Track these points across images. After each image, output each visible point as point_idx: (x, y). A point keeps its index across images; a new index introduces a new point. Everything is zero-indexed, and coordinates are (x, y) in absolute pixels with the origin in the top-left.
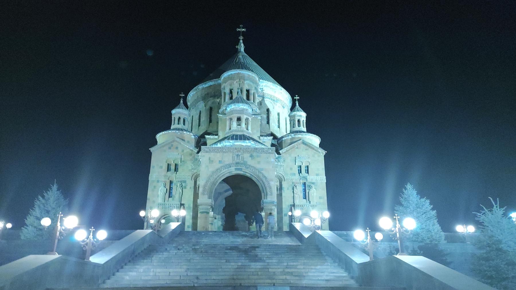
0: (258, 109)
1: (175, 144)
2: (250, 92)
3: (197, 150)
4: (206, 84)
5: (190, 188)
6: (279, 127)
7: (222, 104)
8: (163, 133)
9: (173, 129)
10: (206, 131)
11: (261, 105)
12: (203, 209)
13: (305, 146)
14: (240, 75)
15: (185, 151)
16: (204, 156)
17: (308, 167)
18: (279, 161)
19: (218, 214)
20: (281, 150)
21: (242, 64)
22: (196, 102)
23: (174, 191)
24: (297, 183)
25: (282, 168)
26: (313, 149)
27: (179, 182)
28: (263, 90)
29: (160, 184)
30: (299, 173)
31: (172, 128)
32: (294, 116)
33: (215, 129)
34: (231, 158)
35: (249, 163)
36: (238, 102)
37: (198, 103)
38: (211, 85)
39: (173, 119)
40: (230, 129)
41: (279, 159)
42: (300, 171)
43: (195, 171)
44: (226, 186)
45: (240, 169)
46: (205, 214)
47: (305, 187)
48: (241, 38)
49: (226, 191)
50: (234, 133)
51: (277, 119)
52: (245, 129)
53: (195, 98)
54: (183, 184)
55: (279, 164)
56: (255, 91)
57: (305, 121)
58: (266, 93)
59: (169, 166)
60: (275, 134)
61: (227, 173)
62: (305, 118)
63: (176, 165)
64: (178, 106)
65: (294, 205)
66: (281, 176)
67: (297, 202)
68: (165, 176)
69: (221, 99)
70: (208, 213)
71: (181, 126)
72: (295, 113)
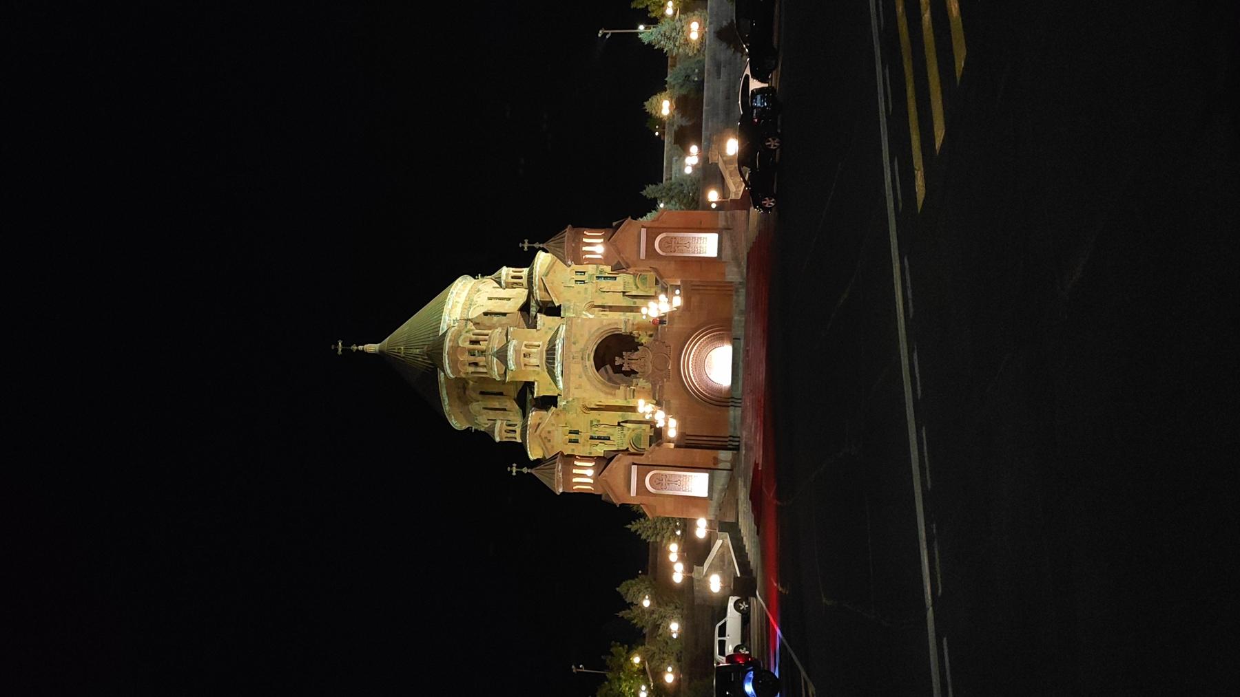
0: (496, 330)
1: (543, 435)
3: (552, 407)
4: (444, 400)
6: (509, 299)
9: (523, 435)
10: (515, 400)
11: (479, 324)
12: (630, 395)
15: (553, 422)
16: (573, 395)
17: (576, 272)
18: (569, 307)
19: (632, 382)
20: (554, 303)
22: (469, 416)
25: (578, 304)
26: (554, 263)
27: (591, 429)
28: (457, 320)
29: (593, 451)
30: (584, 283)
31: (519, 440)
32: (506, 283)
33: (512, 388)
34: (576, 365)
35: (582, 347)
36: (507, 356)
37: (470, 412)
38: (447, 394)
40: (538, 366)
41: (566, 306)
42: (583, 282)
43: (579, 410)
45: (589, 355)
46: (635, 393)
47: (601, 277)
48: (354, 348)
50: (544, 362)
52: (539, 349)
53: (462, 415)
54: (594, 423)
55: (572, 307)
56: (471, 333)
57: (514, 269)
59: (571, 441)
60: (520, 305)
62: (509, 268)
63: (571, 432)
65: (624, 292)
67: (621, 288)
68: (584, 446)
69: (469, 379)
70: (634, 390)
71: (518, 430)
72: (502, 282)
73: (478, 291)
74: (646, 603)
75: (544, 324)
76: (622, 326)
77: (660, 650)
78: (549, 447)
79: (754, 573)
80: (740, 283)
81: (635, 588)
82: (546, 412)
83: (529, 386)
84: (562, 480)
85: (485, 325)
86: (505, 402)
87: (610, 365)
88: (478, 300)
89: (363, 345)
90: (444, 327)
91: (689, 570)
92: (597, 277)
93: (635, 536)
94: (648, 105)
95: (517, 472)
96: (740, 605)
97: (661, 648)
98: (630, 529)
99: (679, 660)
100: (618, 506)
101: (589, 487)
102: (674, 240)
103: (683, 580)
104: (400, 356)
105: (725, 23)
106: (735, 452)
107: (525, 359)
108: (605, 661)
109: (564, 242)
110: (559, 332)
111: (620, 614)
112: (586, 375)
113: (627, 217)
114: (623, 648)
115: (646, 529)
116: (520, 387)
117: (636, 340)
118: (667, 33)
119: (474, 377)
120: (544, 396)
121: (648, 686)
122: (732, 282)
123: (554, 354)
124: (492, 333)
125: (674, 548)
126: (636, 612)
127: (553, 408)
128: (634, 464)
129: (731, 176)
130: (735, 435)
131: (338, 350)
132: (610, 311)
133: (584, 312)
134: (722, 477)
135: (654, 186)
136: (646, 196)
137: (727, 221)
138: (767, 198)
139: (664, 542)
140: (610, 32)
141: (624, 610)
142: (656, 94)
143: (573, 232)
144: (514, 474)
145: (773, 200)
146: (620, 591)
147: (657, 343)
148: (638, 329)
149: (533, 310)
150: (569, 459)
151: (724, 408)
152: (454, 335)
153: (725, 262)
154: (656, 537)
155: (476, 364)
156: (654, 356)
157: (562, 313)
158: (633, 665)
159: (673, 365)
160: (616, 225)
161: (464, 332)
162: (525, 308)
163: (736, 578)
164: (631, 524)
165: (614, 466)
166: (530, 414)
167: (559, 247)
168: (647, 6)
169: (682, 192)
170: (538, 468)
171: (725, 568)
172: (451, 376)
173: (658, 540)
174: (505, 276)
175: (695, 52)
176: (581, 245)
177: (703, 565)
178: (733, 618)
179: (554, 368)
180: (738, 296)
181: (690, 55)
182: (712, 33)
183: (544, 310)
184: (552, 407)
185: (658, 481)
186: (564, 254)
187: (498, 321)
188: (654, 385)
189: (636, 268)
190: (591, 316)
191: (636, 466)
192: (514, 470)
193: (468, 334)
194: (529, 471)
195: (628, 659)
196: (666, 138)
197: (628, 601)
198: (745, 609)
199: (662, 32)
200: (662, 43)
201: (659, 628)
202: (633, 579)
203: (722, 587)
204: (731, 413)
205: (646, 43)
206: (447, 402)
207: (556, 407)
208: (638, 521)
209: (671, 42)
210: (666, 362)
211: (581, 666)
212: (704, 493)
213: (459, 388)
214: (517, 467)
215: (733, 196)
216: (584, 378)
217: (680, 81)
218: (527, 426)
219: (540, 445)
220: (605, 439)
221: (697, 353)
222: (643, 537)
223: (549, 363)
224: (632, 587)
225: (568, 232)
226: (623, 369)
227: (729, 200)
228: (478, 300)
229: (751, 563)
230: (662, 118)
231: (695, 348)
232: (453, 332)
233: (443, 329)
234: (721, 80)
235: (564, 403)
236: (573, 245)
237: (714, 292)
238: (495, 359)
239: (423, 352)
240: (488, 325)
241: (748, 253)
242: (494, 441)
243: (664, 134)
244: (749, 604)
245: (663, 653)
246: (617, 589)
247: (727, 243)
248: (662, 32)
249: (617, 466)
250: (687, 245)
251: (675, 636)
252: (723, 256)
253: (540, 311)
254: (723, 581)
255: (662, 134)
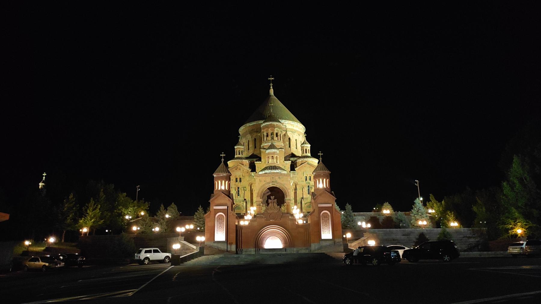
0: (283, 144)
1: (238, 167)
2: (278, 134)
3: (251, 170)
4: (251, 123)
5: (249, 190)
6: (296, 148)
7: (263, 142)
8: (232, 161)
10: (253, 153)
11: (285, 136)
13: (309, 165)
14: (272, 125)
15: (244, 171)
17: (310, 177)
18: (295, 174)
20: (296, 168)
21: (273, 116)
22: (245, 135)
23: (240, 193)
24: (305, 186)
25: (296, 178)
26: (314, 167)
28: (286, 126)
30: (306, 181)
31: (236, 156)
35: (278, 181)
37: (247, 135)
38: (254, 125)
39: (236, 151)
41: (295, 173)
42: (306, 180)
43: (250, 181)
44: (268, 190)
45: (274, 184)
46: (259, 206)
47: (309, 188)
48: (271, 85)
49: (268, 193)
51: (296, 144)
52: (276, 163)
53: (245, 131)
54: (245, 189)
55: (295, 176)
58: (288, 128)
59: (236, 179)
61: (268, 186)
63: (240, 178)
64: (238, 144)
65: (303, 198)
66: (296, 182)
67: (304, 197)
68: (235, 185)
69: (261, 133)
71: (240, 156)
73: (299, 135)
74: (167, 216)
75: (287, 164)
76: (288, 198)
77: (147, 224)
78: (234, 169)
79: (182, 264)
80: (311, 250)
81: (174, 211)
82: (248, 167)
83: (260, 159)
84: (219, 176)
85: (284, 139)
86: (252, 150)
87: (271, 194)
88: (295, 135)
89: (273, 88)
90: (283, 121)
91: (183, 234)
92: (309, 186)
93: (196, 210)
94: (386, 204)
95: (222, 156)
96: (168, 259)
97: (148, 224)
98: (199, 207)
99: (142, 232)
100: (209, 201)
101: (217, 188)
102: (327, 219)
103: (178, 232)
104: (269, 103)
105: (427, 237)
106: (235, 252)
107: (271, 157)
108: (142, 200)
109: (323, 170)
110: (283, 171)
111: (162, 205)
112: (265, 184)
113: (336, 198)
114: (148, 207)
115: (199, 214)
116: (258, 155)
117: (282, 205)
118: (420, 211)
119: (262, 135)
120: (255, 166)
121: (131, 219)
122: (311, 246)
123: (274, 169)
124: (281, 142)
125: (191, 227)
126: (163, 212)
127: (250, 170)
128: (228, 207)
129: (359, 243)
130: (243, 252)
131: (270, 78)
132: (294, 192)
133: (293, 181)
134: (224, 247)
135: (351, 209)
136: (346, 205)
137: (338, 242)
138: (350, 260)
139: (194, 223)
140: (418, 185)
141: (164, 207)
142: (392, 207)
143: (327, 174)
144: (221, 155)
145: (349, 263)
146: (172, 204)
147: (281, 214)
148: (287, 205)
149: (292, 159)
150: (228, 178)
151: (254, 245)
152: (280, 126)
153: (320, 242)
154: (196, 219)
155: (267, 136)
156: (276, 213)
157: (292, 171)
158: (140, 212)
159: (272, 222)
160: (332, 193)
161: (280, 130)
162: (293, 155)
163: (179, 256)
164: (202, 207)
165: (227, 199)
166: (247, 161)
167: (320, 169)
168: (431, 201)
169: (349, 221)
170: (224, 165)
171: (184, 251)
172: (262, 126)
173: (195, 220)
174: (306, 146)
175: (413, 224)
176: (322, 178)
177: (185, 240)
178: (161, 256)
179: (268, 169)
180: (305, 250)
181: (411, 222)
182: (422, 231)
183: (292, 163)
184: (251, 170)
185: (220, 218)
186: (318, 171)
187: (287, 144)
188: (263, 214)
189: (314, 203)
190: (291, 184)
191: (227, 208)
192: (223, 155)
193: (280, 131)
194: (222, 162)
195: (142, 210)
196: (373, 213)
197: (168, 208)
198: (166, 261)
199: (420, 209)
200: (416, 209)
201: (157, 223)
202: (178, 210)
203: (175, 249)
204: (253, 250)
205: (414, 201)
206: (250, 125)
207: (251, 171)
208: (203, 210)
209: (416, 213)
210: (273, 219)
211: (139, 189)
212: (216, 239)
213: (257, 129)
214: (224, 156)
215: (349, 245)
216: (265, 183)
217: (399, 217)
218: (242, 159)
219: (234, 166)
220: (238, 194)
221: (278, 232)
222: (196, 213)
223: (270, 167)
224: (174, 209)
225: (328, 172)
226: (269, 200)
227: (348, 243)
228: (295, 135)
229: (186, 263)
230: (382, 211)
231: (280, 231)
232: (280, 125)
233: (282, 121)
234: (402, 236)
235: (253, 175)
236: (322, 175)
237: (306, 239)
238: (270, 144)
239: (271, 113)
240: (285, 140)
241: (324, 253)
242: (235, 146)
243: (374, 212)
244: (168, 263)
245: (146, 225)
246: (173, 203)
247: (328, 243)
248: (420, 209)
249: (227, 200)
250: (326, 225)
251: (153, 230)
252: (322, 242)
253: (292, 162)
254: (178, 250)
255: (375, 211)
